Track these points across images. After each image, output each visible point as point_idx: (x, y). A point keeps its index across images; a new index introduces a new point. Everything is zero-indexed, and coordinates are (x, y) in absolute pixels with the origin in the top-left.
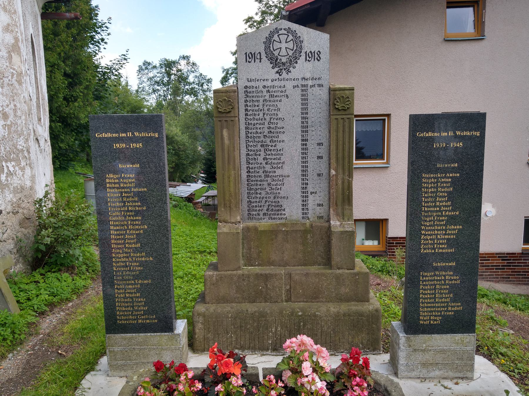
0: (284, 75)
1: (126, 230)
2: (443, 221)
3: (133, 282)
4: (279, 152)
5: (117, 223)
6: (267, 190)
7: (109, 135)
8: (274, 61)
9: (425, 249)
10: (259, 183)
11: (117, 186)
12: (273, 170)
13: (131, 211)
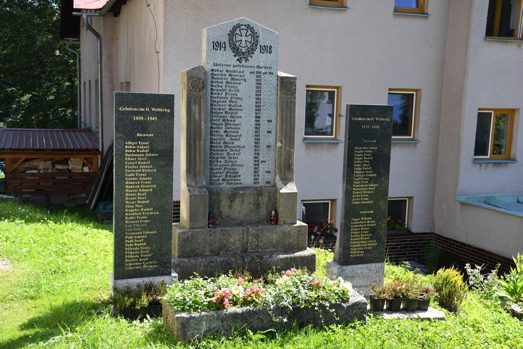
0: (243, 62)
1: (138, 189)
2: (366, 180)
3: (141, 233)
4: (237, 126)
5: (132, 183)
6: (227, 158)
7: (131, 109)
8: (236, 51)
9: (355, 201)
10: (220, 152)
11: (134, 151)
12: (232, 141)
13: (144, 173)
